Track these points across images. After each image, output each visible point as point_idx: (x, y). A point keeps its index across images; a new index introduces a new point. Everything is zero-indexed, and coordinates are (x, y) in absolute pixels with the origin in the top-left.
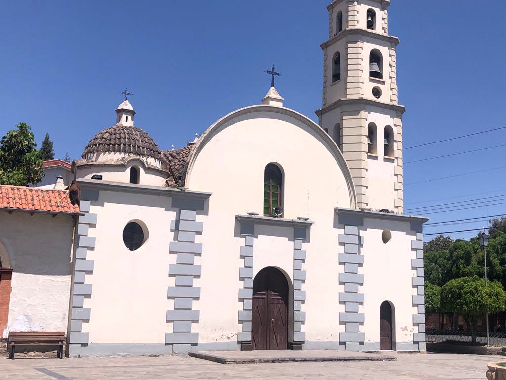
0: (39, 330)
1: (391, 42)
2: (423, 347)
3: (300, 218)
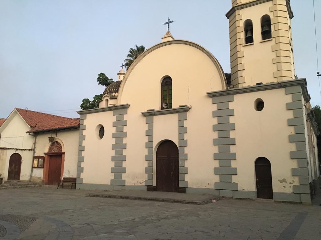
2: (307, 198)
3: (180, 107)
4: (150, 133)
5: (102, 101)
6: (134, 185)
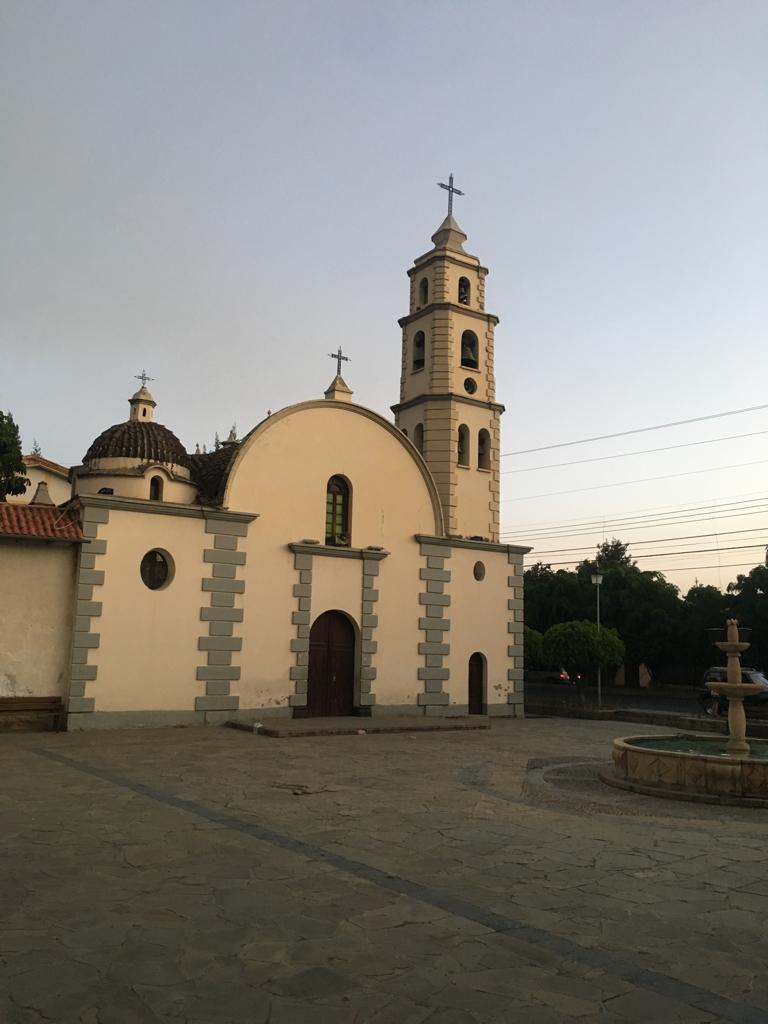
0: (27, 695)
1: (489, 321)
3: (370, 548)
4: (302, 592)
5: (143, 477)
6: (260, 707)
